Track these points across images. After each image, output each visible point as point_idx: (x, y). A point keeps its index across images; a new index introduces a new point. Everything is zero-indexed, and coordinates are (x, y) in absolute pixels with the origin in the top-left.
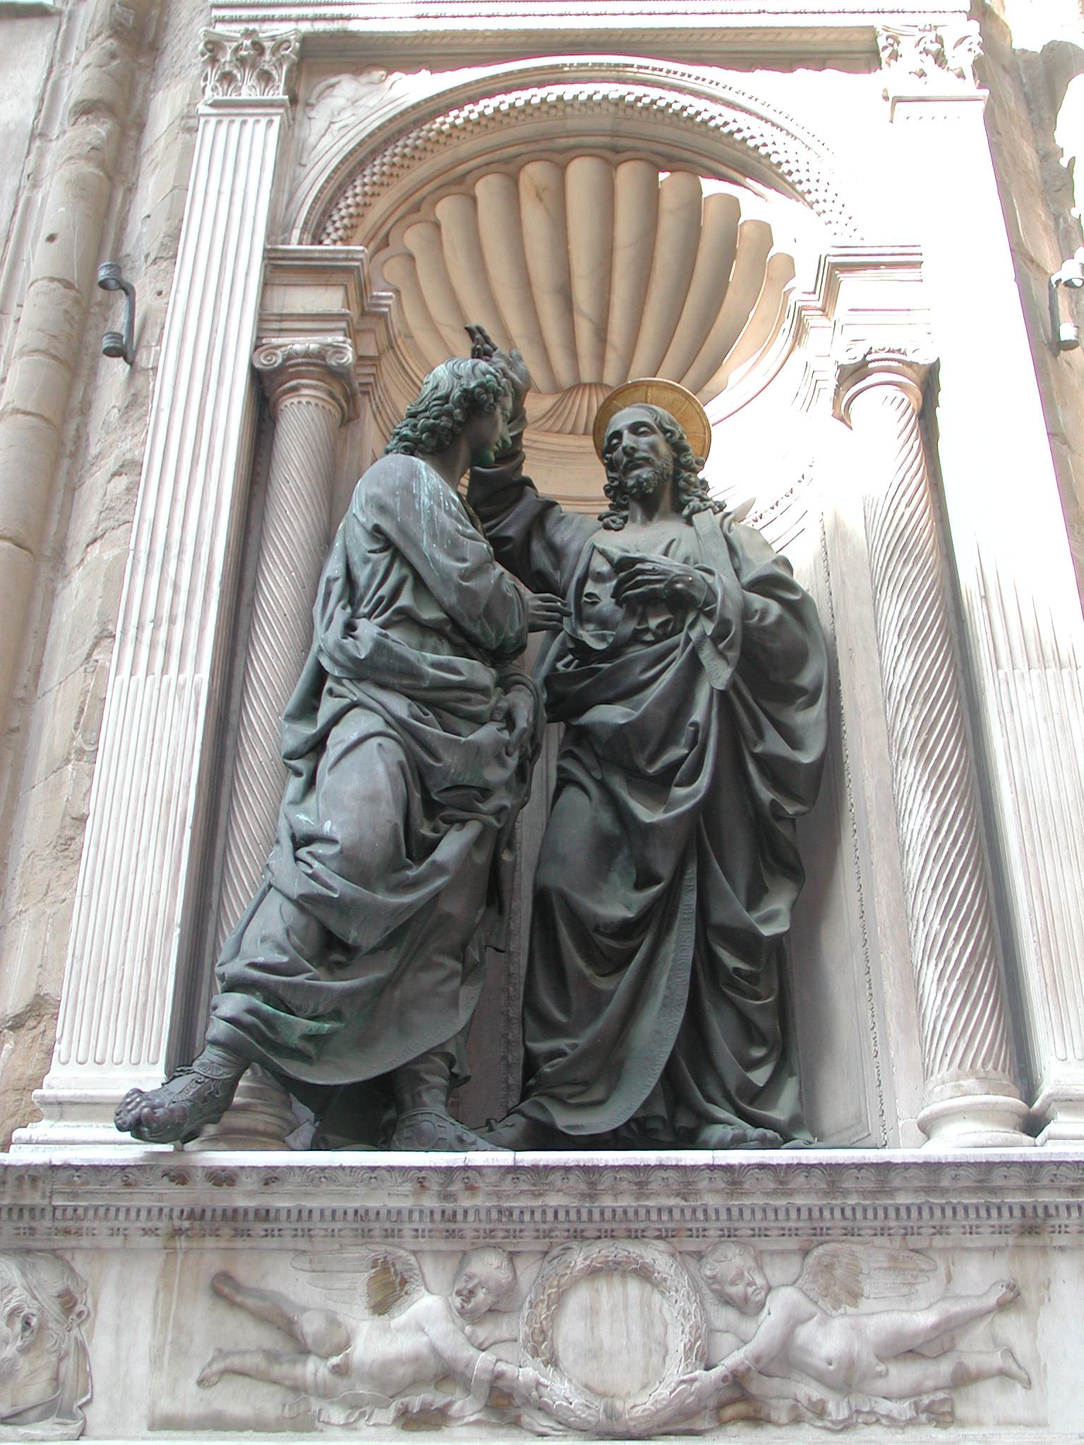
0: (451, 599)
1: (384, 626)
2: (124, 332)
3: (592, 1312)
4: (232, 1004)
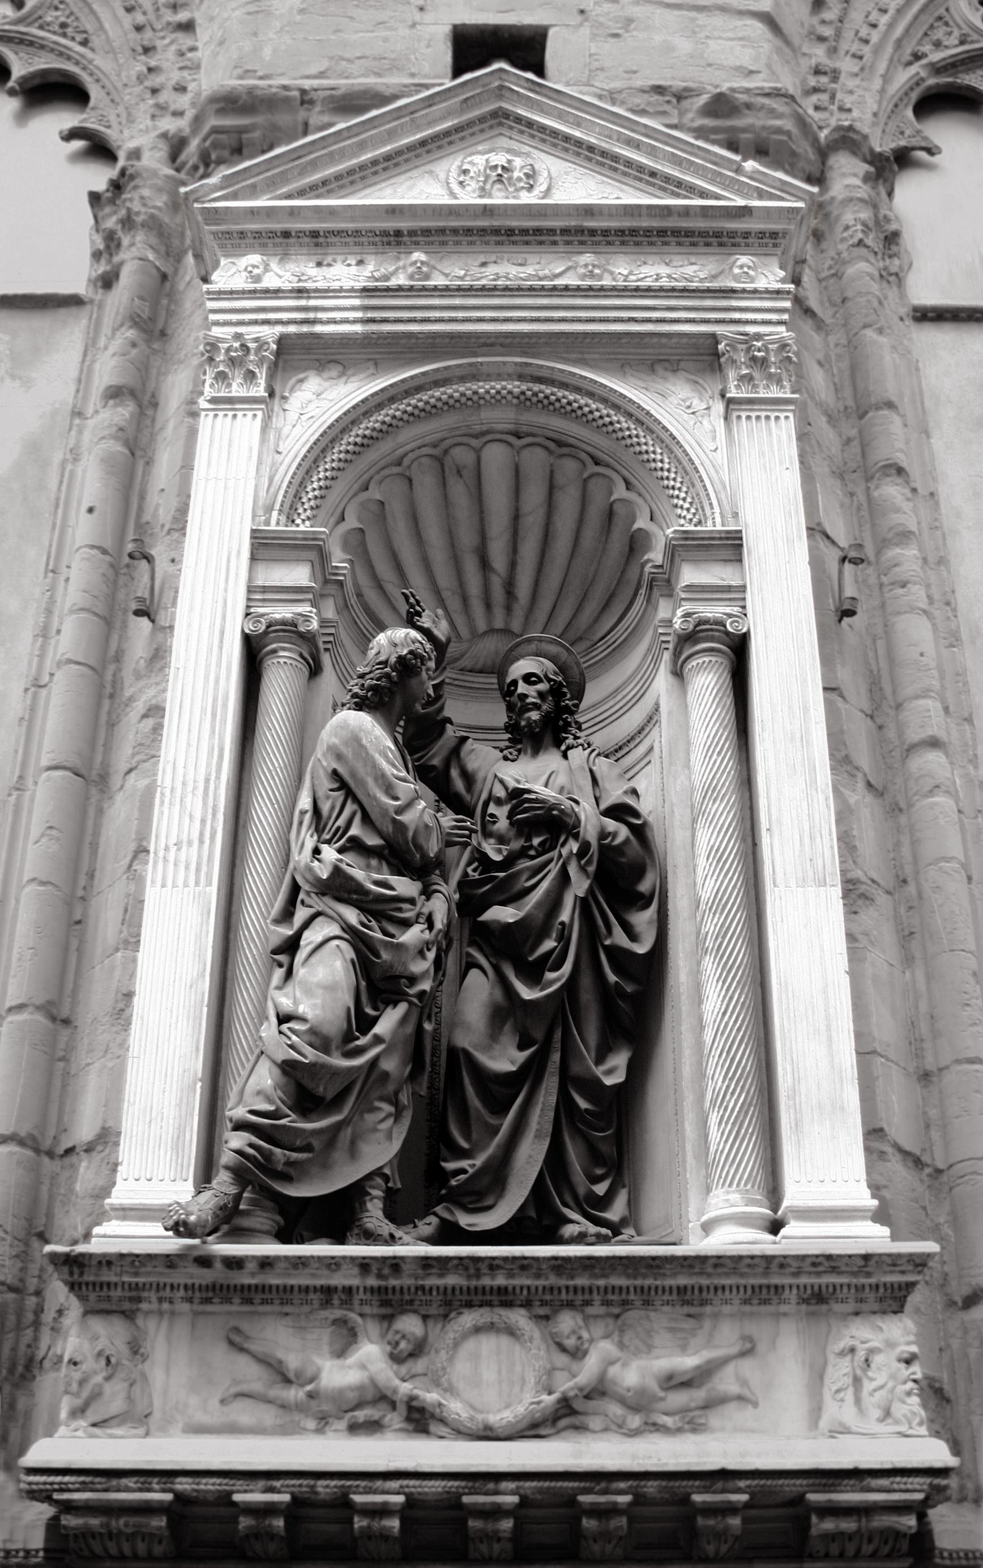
2: (147, 595)
3: (476, 1357)
4: (238, 1140)
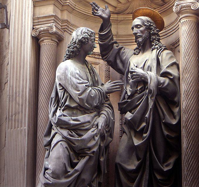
0: (78, 101)
1: (63, 111)
